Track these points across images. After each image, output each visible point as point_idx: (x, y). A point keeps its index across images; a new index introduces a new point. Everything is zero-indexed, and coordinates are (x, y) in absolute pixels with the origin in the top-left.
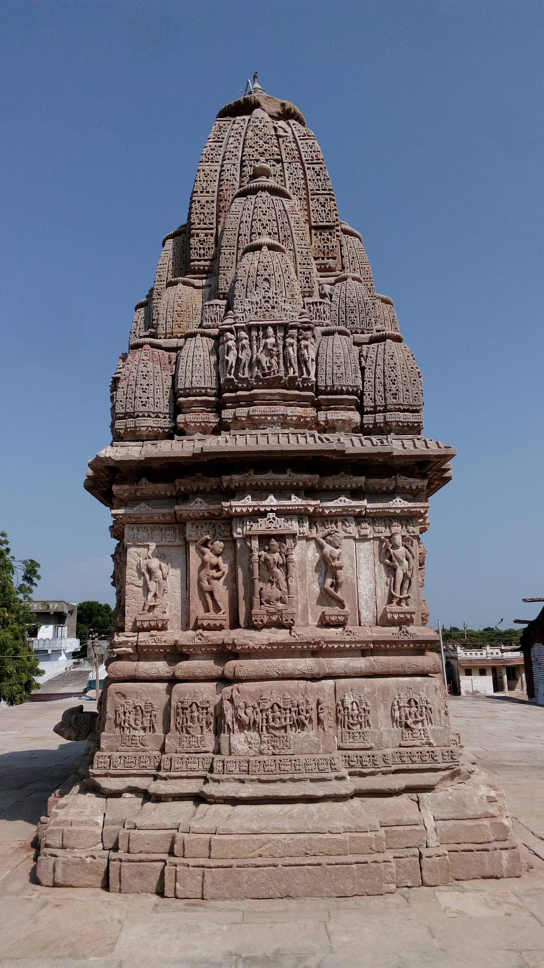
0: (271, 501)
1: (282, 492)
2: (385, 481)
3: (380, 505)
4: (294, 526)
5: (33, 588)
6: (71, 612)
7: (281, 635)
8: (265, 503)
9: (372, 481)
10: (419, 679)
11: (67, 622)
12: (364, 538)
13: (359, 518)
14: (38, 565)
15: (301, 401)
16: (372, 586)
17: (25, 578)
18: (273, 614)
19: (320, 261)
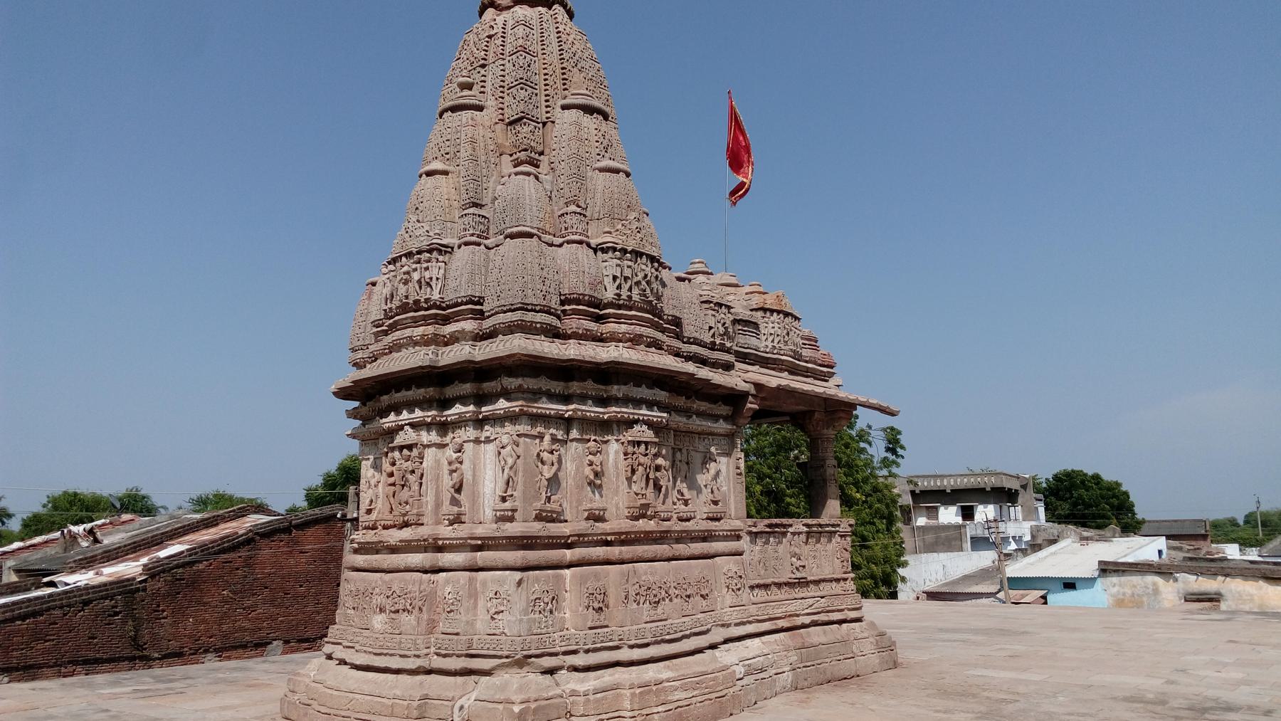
0: (405, 415)
1: (410, 406)
2: (493, 384)
3: (490, 408)
4: (426, 437)
5: (899, 460)
6: (1024, 487)
7: (406, 534)
8: (401, 417)
9: (486, 385)
10: (507, 572)
11: (1020, 500)
12: (488, 441)
13: (480, 423)
14: (899, 433)
15: (425, 320)
16: (492, 485)
17: (888, 449)
18: (404, 515)
19: (515, 156)
